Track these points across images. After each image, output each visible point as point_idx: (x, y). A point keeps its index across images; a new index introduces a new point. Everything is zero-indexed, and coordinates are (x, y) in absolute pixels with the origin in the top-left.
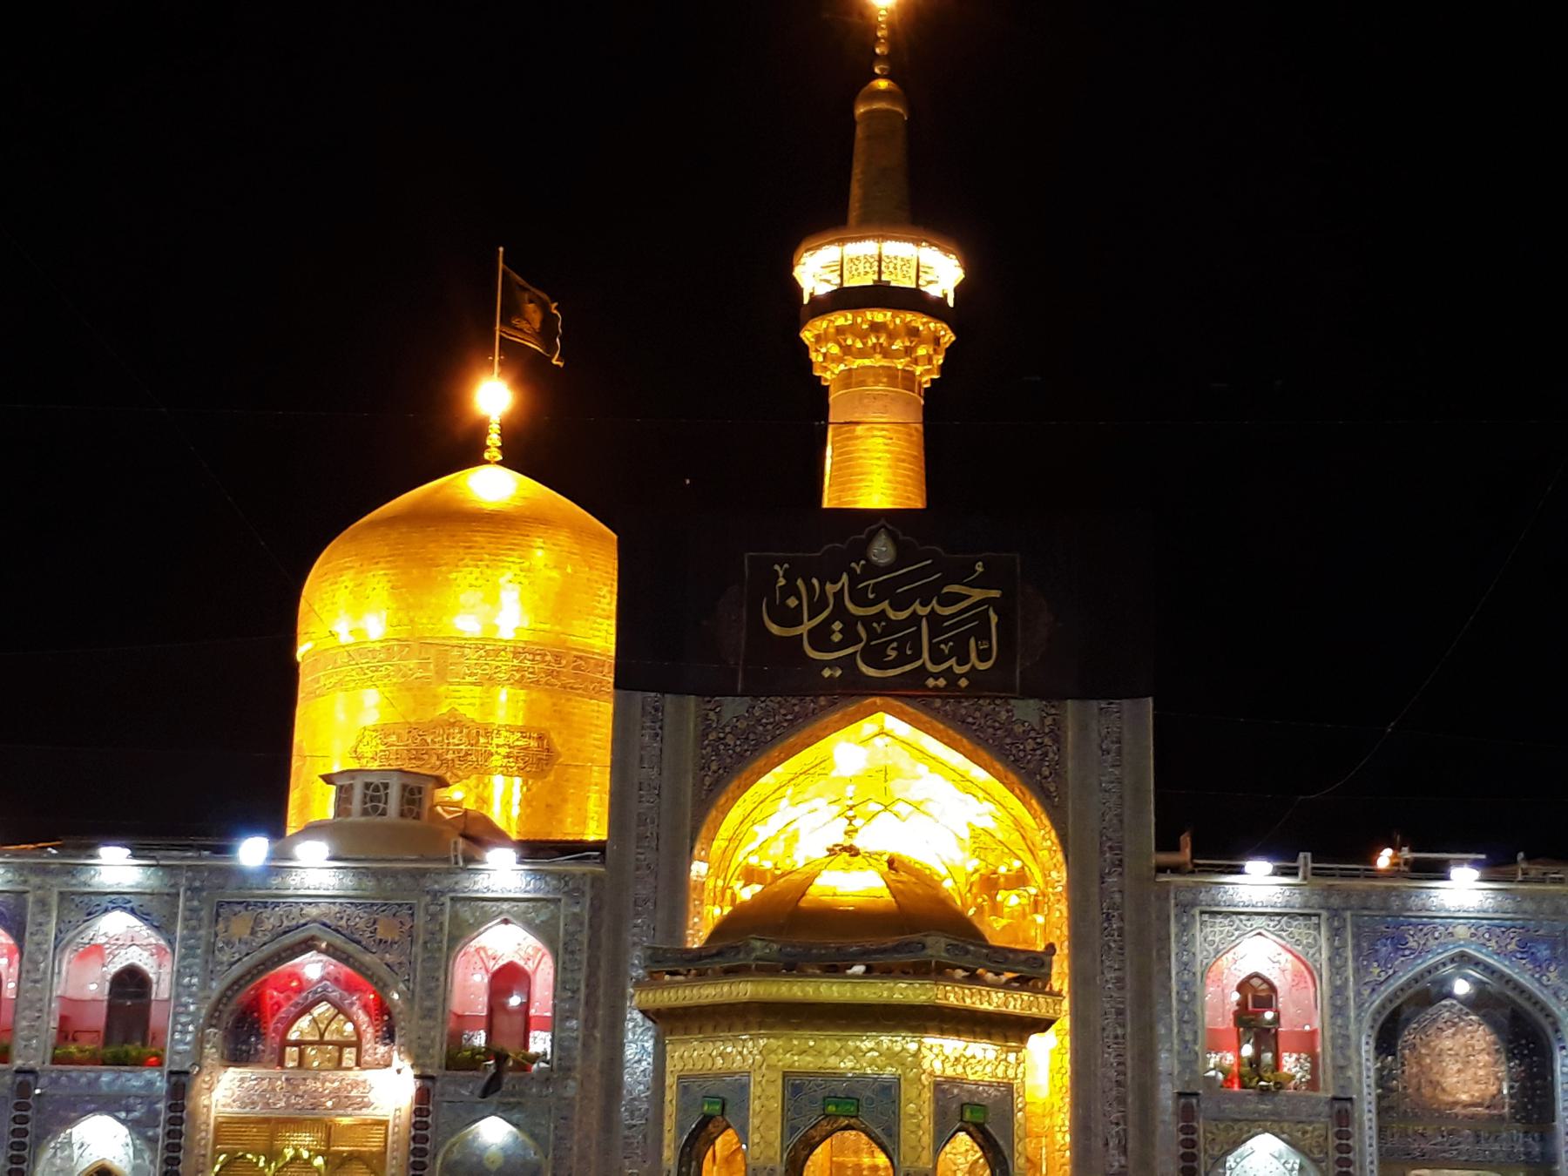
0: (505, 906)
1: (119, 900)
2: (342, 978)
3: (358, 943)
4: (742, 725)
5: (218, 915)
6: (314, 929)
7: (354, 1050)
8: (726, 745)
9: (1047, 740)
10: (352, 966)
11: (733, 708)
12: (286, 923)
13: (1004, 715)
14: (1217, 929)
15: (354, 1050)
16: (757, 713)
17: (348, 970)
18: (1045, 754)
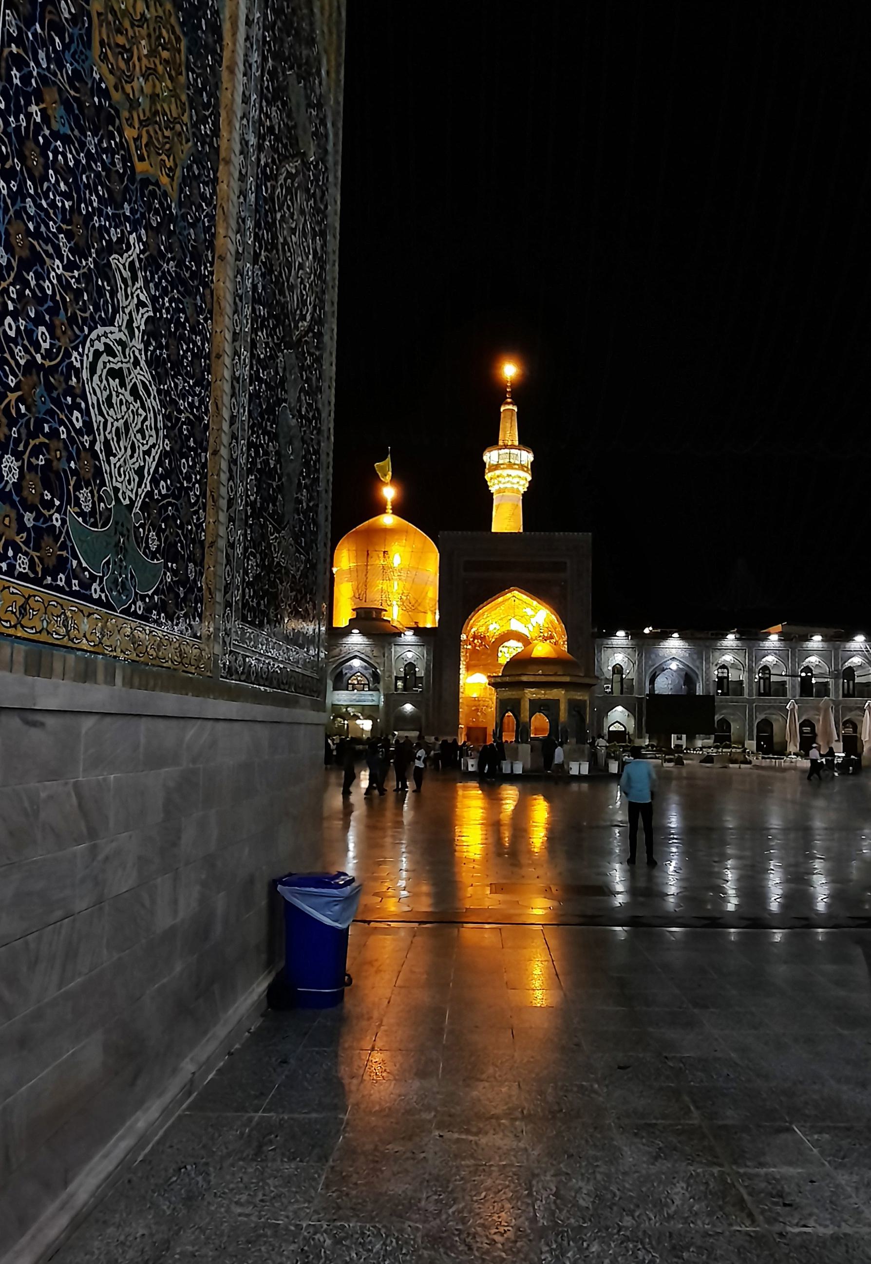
6: (357, 654)
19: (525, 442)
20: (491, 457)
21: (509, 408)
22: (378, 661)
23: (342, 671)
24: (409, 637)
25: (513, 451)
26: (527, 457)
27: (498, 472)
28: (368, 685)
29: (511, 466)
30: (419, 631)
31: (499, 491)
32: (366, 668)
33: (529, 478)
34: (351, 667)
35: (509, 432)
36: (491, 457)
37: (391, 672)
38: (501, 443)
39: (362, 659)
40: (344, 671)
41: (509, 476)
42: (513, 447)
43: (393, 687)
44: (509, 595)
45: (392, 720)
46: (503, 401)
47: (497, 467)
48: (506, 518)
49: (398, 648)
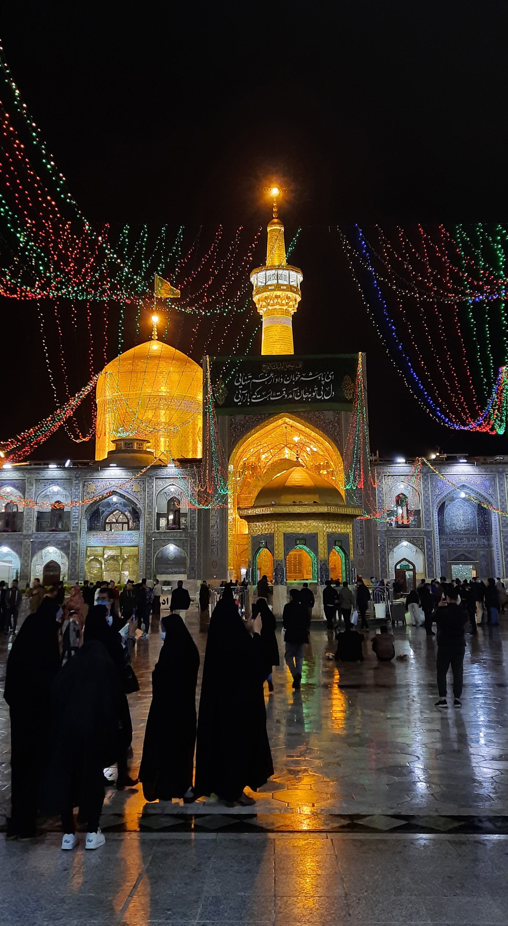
0: (172, 480)
1: (53, 481)
2: (122, 503)
3: (128, 492)
4: (242, 422)
5: (84, 485)
7: (127, 525)
8: (238, 429)
9: (336, 425)
10: (126, 499)
11: (239, 418)
12: (105, 487)
13: (322, 417)
14: (390, 480)
15: (127, 525)
16: (247, 418)
17: (124, 500)
18: (336, 429)
19: (293, 261)
20: (257, 278)
21: (275, 230)
22: (139, 497)
23: (98, 509)
24: (172, 470)
25: (280, 272)
26: (296, 278)
27: (266, 294)
28: (128, 523)
29: (278, 287)
30: (184, 463)
31: (269, 313)
32: (125, 505)
33: (299, 299)
34: (109, 505)
35: (276, 252)
36: (257, 278)
37: (150, 506)
38: (268, 263)
39: (121, 496)
40: (101, 509)
41: (277, 297)
42: (280, 267)
43: (154, 525)
44: (280, 422)
45: (153, 564)
46: (268, 221)
47: (266, 288)
48: (277, 340)
49: (160, 482)
